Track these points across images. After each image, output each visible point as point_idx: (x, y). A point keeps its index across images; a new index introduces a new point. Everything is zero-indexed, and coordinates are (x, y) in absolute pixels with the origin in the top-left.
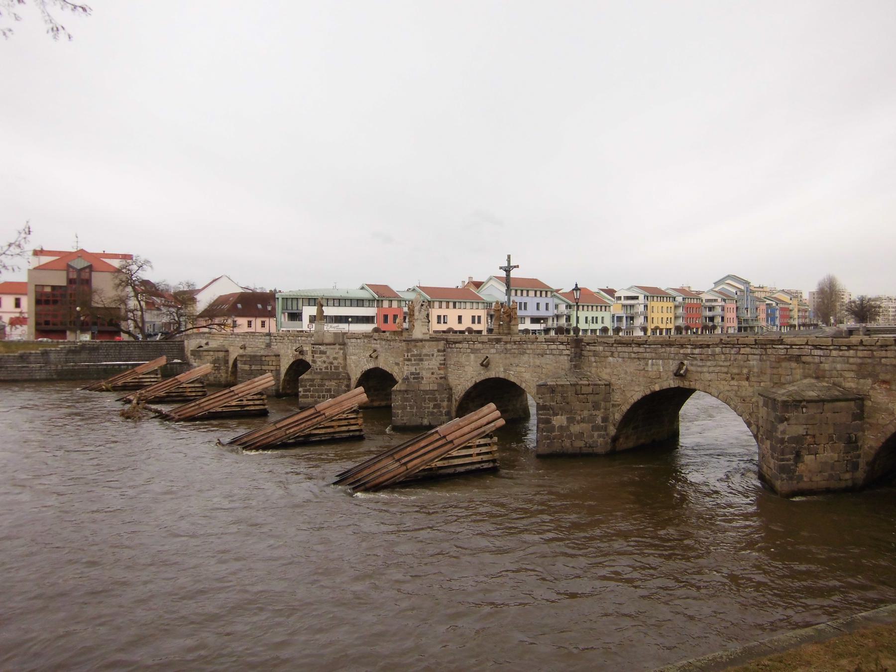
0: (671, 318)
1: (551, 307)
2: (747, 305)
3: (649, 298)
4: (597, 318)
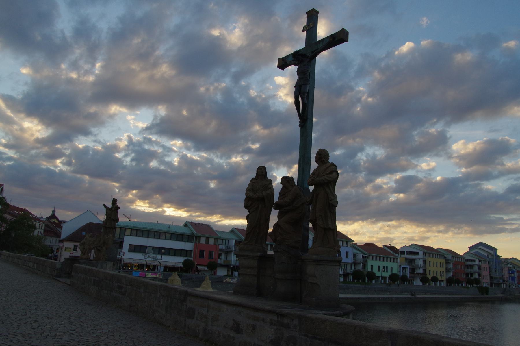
0: (443, 272)
1: (350, 256)
2: (496, 266)
3: (427, 254)
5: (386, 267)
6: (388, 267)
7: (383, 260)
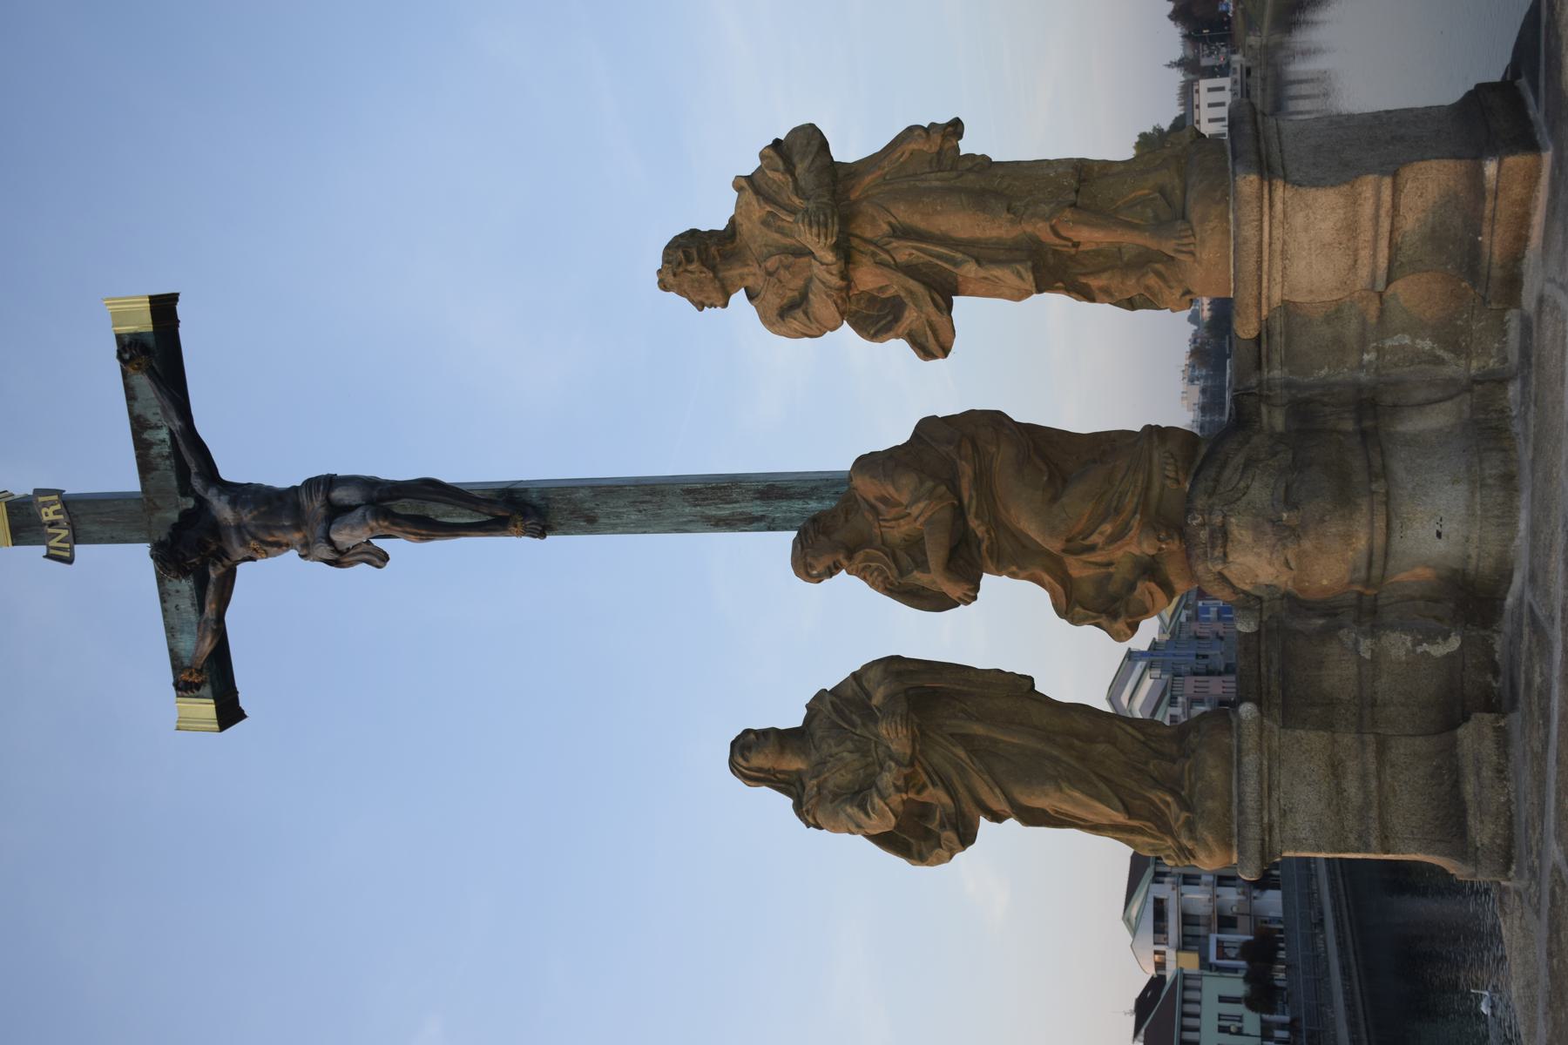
2: (1189, 655)
4: (1220, 1017)
5: (1219, 1019)
6: (1220, 1015)
7: (1197, 1030)
